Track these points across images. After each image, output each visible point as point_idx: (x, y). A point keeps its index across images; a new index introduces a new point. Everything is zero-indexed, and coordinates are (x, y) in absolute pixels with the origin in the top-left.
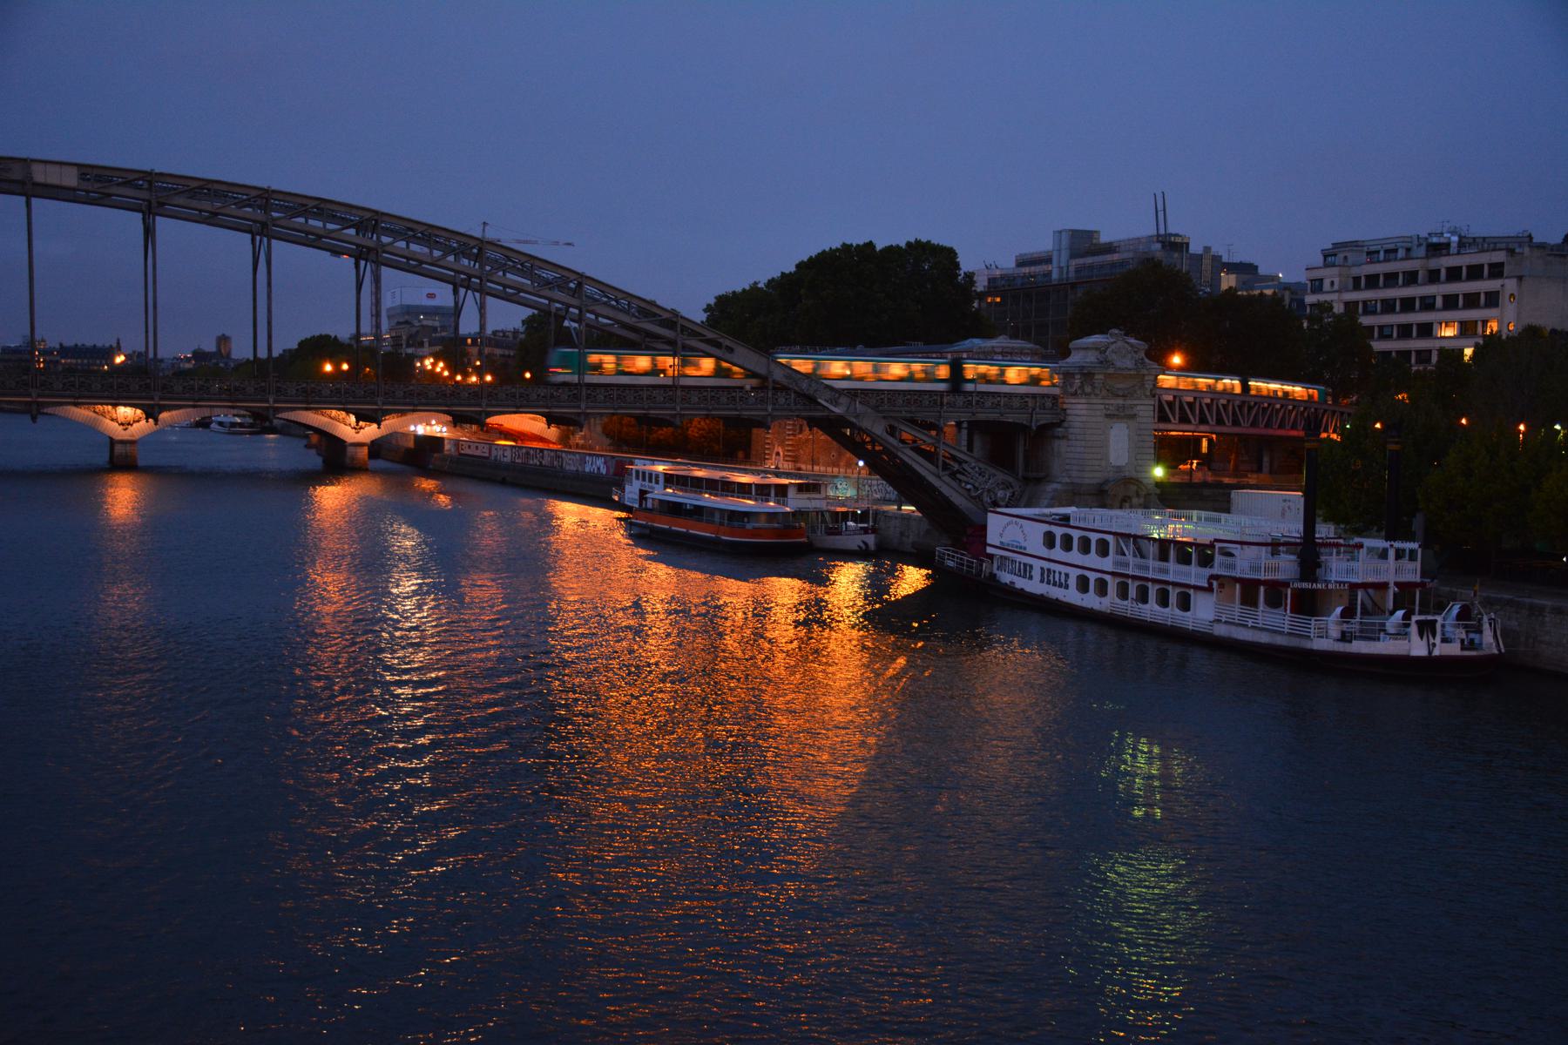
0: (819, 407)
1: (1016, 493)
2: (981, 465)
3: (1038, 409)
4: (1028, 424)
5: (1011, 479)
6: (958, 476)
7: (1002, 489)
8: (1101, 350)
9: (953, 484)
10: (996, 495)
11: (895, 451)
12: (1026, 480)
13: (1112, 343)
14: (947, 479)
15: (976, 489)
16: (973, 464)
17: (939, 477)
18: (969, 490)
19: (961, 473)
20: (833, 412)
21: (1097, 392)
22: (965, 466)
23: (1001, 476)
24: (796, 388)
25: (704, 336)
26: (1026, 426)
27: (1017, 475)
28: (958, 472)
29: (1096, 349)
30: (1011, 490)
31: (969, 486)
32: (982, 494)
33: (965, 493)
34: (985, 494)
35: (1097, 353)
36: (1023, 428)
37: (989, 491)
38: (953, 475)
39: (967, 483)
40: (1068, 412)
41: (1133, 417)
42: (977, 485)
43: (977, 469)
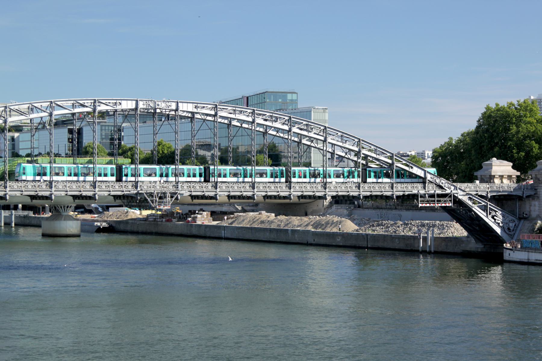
3: (525, 189)
4: (522, 195)
5: (514, 218)
7: (512, 223)
9: (493, 220)
10: (509, 225)
17: (487, 217)
19: (497, 216)
22: (497, 213)
26: (519, 196)
27: (516, 216)
28: (495, 216)
30: (515, 223)
37: (506, 223)
38: (493, 217)
40: (538, 190)
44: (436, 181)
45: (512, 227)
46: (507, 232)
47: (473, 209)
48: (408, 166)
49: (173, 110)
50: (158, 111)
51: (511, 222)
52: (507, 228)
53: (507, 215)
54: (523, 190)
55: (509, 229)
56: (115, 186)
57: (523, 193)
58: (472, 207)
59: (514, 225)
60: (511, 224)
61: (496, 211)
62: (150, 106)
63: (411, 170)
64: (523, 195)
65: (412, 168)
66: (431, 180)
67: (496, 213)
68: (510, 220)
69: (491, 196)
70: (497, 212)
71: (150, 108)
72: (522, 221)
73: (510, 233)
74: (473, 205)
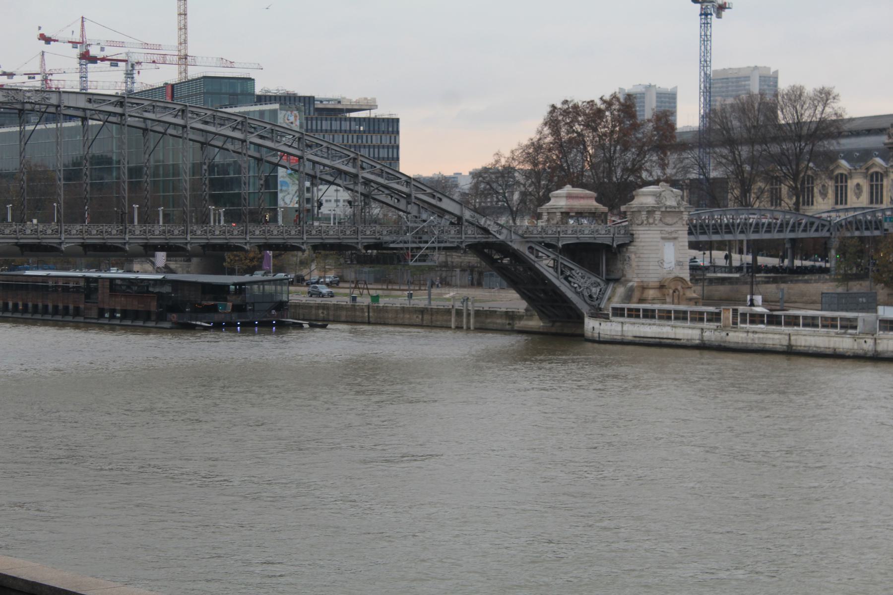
0: (491, 236)
1: (602, 290)
2: (583, 272)
3: (616, 235)
4: (611, 244)
5: (599, 280)
6: (570, 279)
7: (595, 287)
8: (658, 196)
10: (591, 291)
11: (533, 263)
12: (608, 281)
13: (663, 191)
14: (563, 281)
15: (580, 287)
16: (578, 271)
17: (558, 278)
18: (576, 288)
19: (572, 277)
20: (498, 238)
21: (657, 222)
22: (573, 272)
23: (594, 279)
24: (477, 224)
25: (425, 191)
26: (608, 246)
27: (602, 276)
28: (569, 276)
29: (654, 195)
30: (600, 288)
31: (576, 285)
32: (583, 290)
33: (573, 290)
34: (585, 290)
35: (654, 198)
36: (608, 248)
37: (587, 288)
38: (566, 278)
39: (574, 283)
40: (635, 236)
41: (675, 238)
42: (580, 284)
43: (580, 274)
44: (478, 222)
45: (595, 293)
46: (589, 302)
47: (537, 265)
48: (434, 197)
49: (53, 105)
50: (28, 107)
51: (595, 285)
52: (587, 295)
53: (588, 275)
54: (612, 236)
55: (591, 296)
56: (25, 230)
57: (613, 241)
58: (534, 262)
59: (598, 290)
60: (594, 290)
61: (571, 269)
62: (14, 98)
63: (439, 204)
64: (613, 243)
65: (440, 200)
66: (471, 219)
67: (571, 272)
68: (593, 282)
69: (563, 246)
70: (573, 270)
71: (14, 101)
72: (611, 286)
73: (594, 303)
74: (536, 259)
